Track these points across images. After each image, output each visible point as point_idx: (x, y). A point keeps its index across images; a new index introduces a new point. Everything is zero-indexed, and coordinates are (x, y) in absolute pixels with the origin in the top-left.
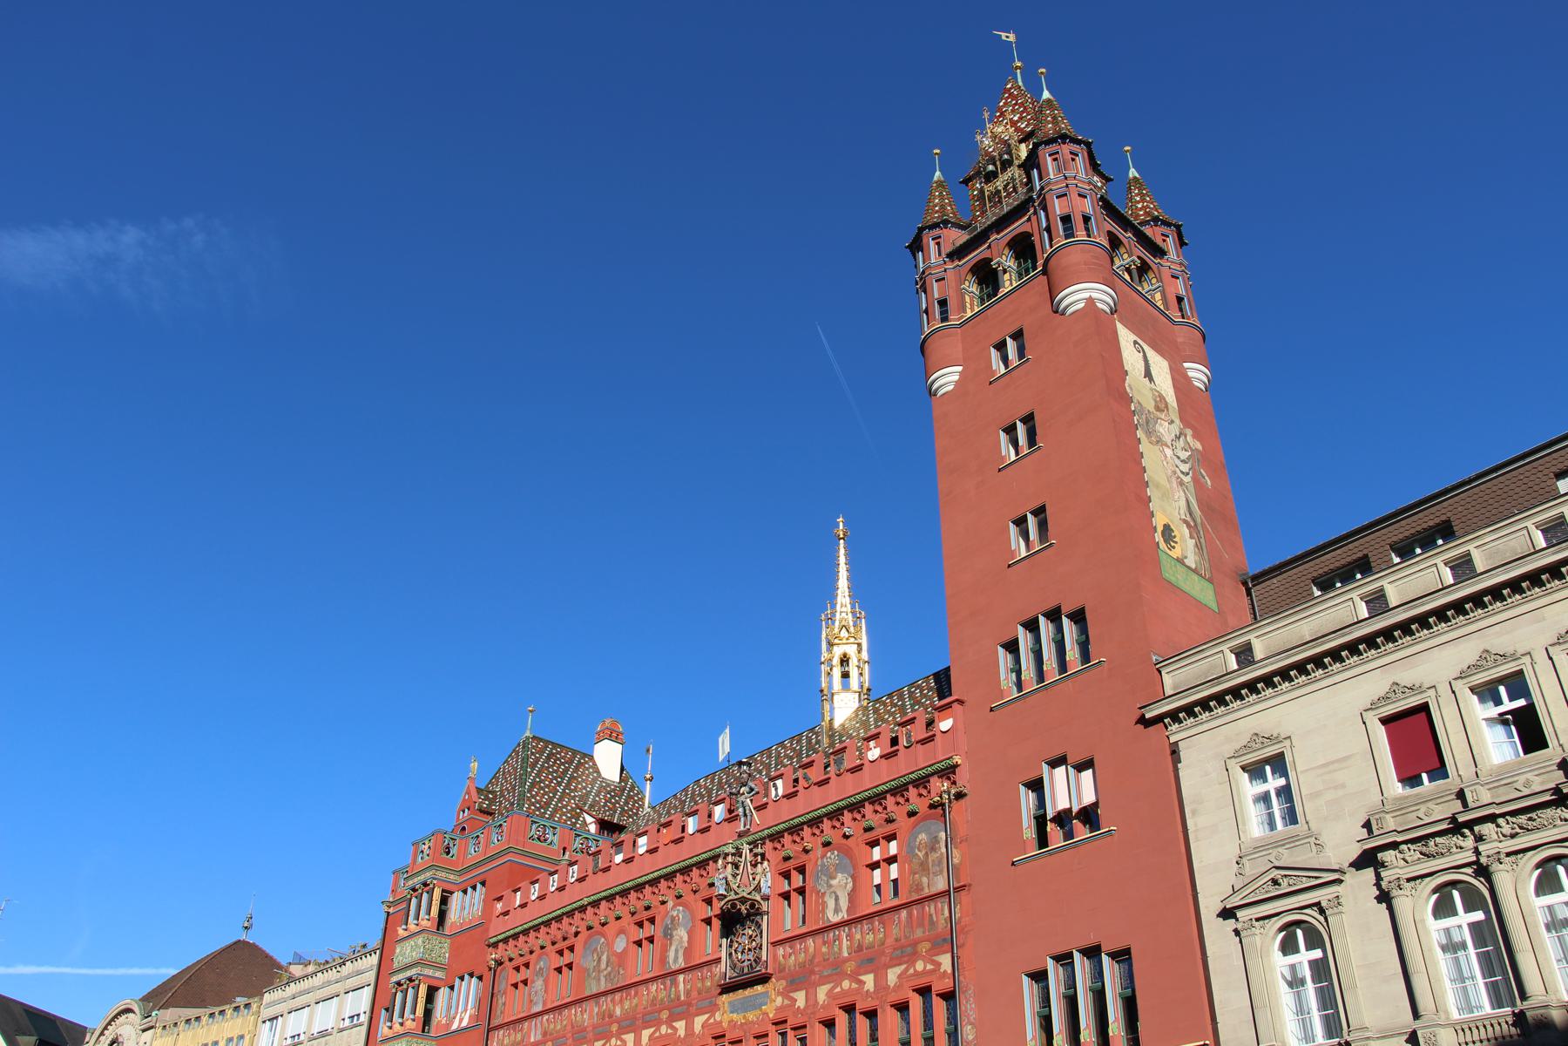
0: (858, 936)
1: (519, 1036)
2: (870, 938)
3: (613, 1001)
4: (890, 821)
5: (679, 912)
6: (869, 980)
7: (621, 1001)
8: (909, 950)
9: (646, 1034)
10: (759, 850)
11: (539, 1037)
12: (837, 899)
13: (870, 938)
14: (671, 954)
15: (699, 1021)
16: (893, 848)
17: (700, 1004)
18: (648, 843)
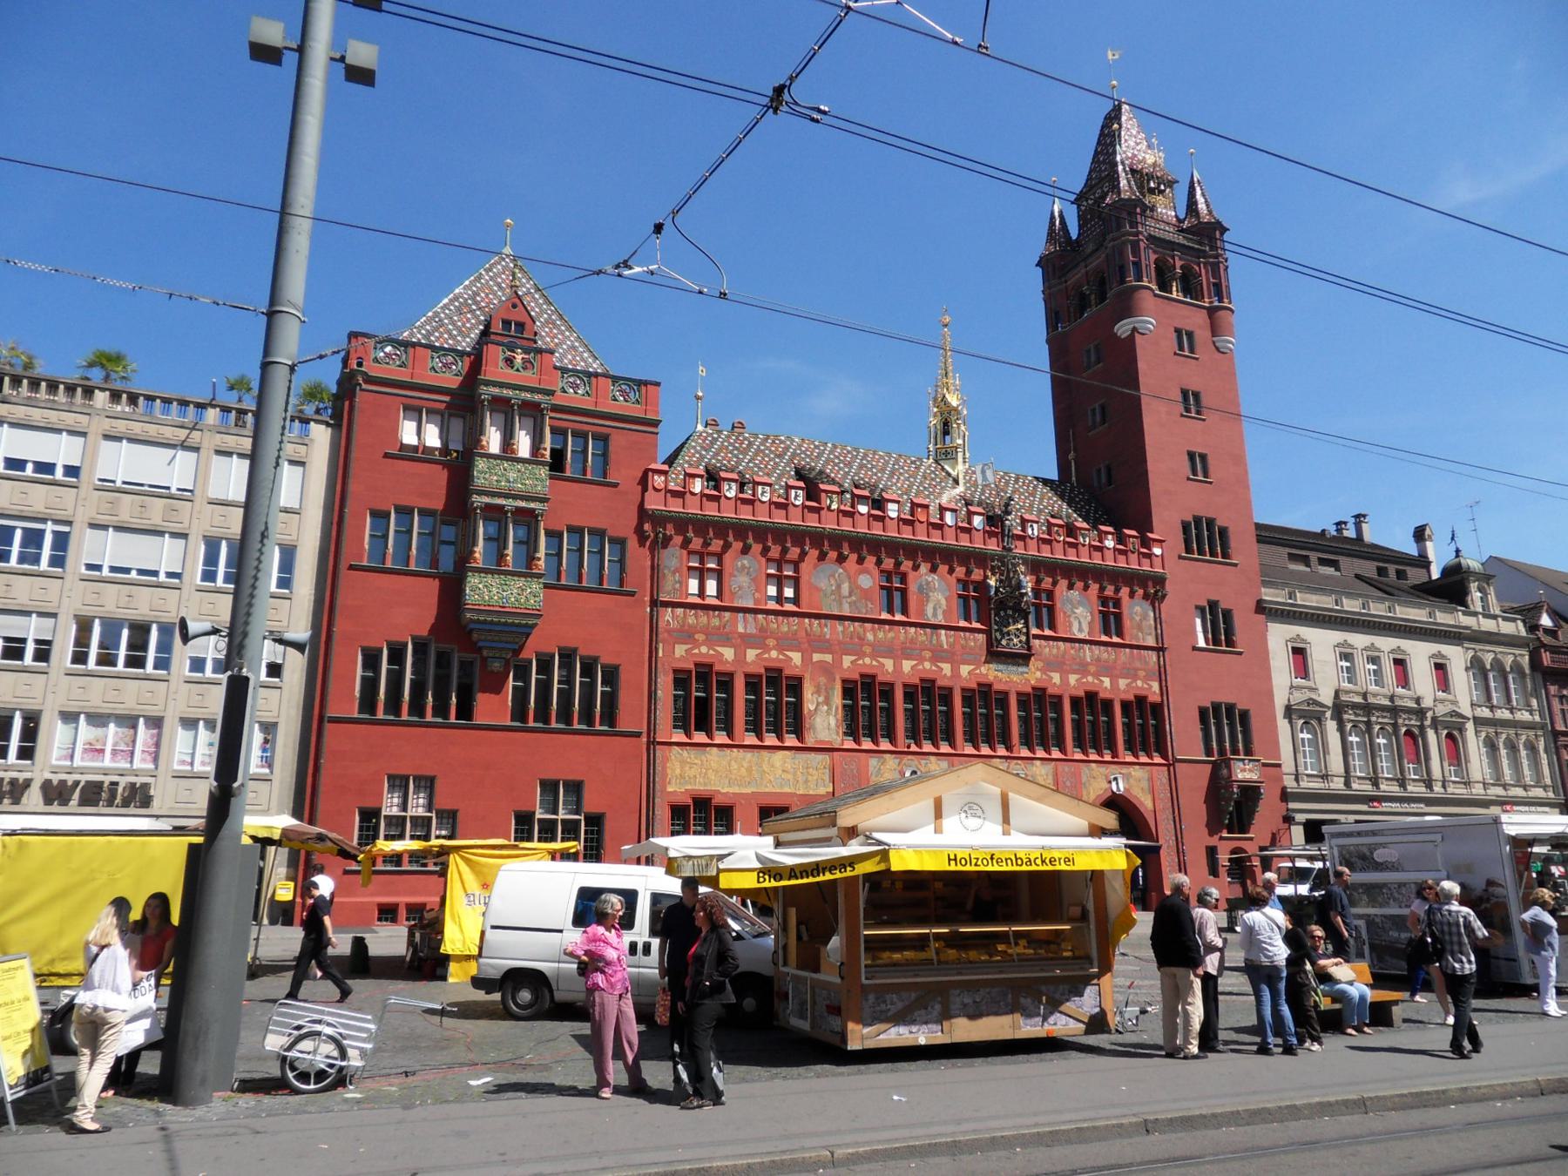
1: (716, 622)
2: (1105, 655)
6: (1107, 682)
9: (907, 665)
11: (752, 630)
13: (1105, 655)
14: (929, 610)
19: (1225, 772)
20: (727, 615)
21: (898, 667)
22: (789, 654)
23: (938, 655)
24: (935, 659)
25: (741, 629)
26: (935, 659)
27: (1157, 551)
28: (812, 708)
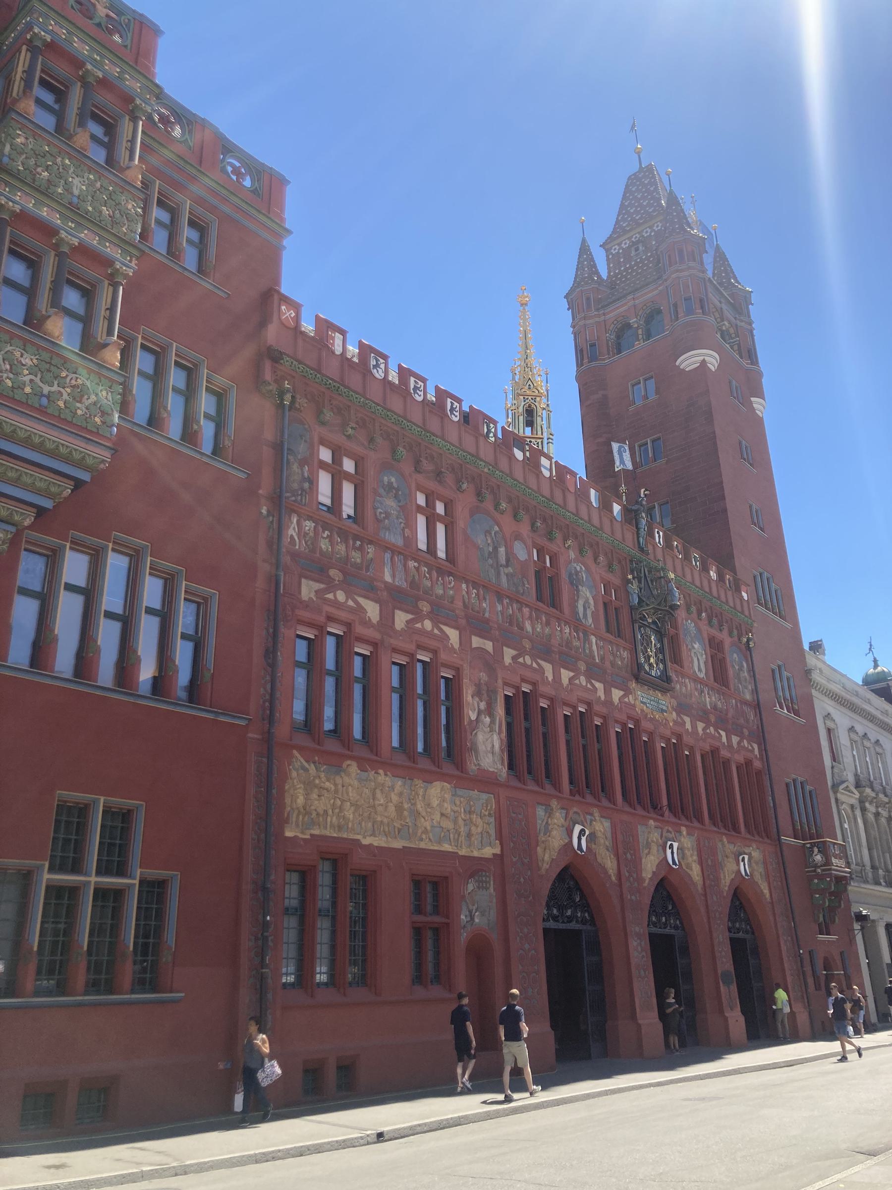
0: (713, 699)
1: (356, 557)
9: (566, 675)
11: (401, 582)
19: (818, 858)
20: (371, 550)
22: (446, 629)
24: (591, 674)
25: (388, 578)
27: (745, 595)
28: (473, 717)
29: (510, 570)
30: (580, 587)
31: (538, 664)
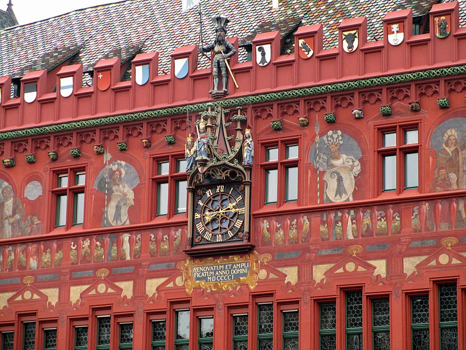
0: (367, 221)
2: (382, 224)
3: (25, 251)
4: (415, 111)
5: (122, 167)
6: (380, 267)
7: (38, 254)
8: (431, 242)
9: (75, 293)
10: (239, 116)
12: (340, 180)
13: (382, 224)
14: (111, 211)
15: (152, 286)
16: (412, 138)
17: (154, 267)
18: (78, 85)
21: (64, 296)
23: (117, 271)
24: (111, 280)
26: (111, 280)
29: (18, 217)
30: (114, 188)
31: (40, 294)
